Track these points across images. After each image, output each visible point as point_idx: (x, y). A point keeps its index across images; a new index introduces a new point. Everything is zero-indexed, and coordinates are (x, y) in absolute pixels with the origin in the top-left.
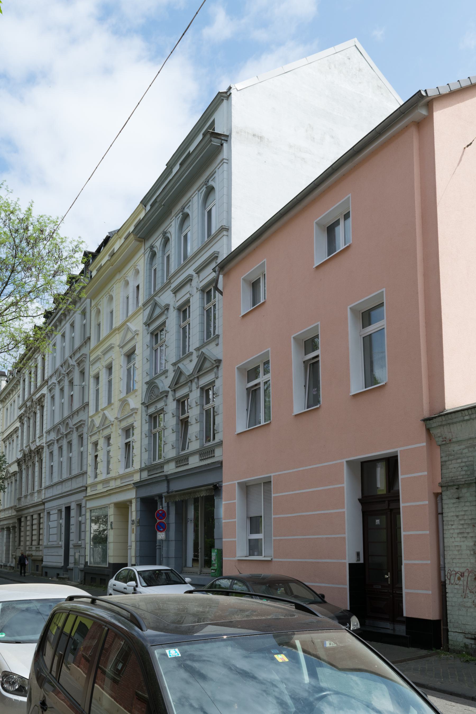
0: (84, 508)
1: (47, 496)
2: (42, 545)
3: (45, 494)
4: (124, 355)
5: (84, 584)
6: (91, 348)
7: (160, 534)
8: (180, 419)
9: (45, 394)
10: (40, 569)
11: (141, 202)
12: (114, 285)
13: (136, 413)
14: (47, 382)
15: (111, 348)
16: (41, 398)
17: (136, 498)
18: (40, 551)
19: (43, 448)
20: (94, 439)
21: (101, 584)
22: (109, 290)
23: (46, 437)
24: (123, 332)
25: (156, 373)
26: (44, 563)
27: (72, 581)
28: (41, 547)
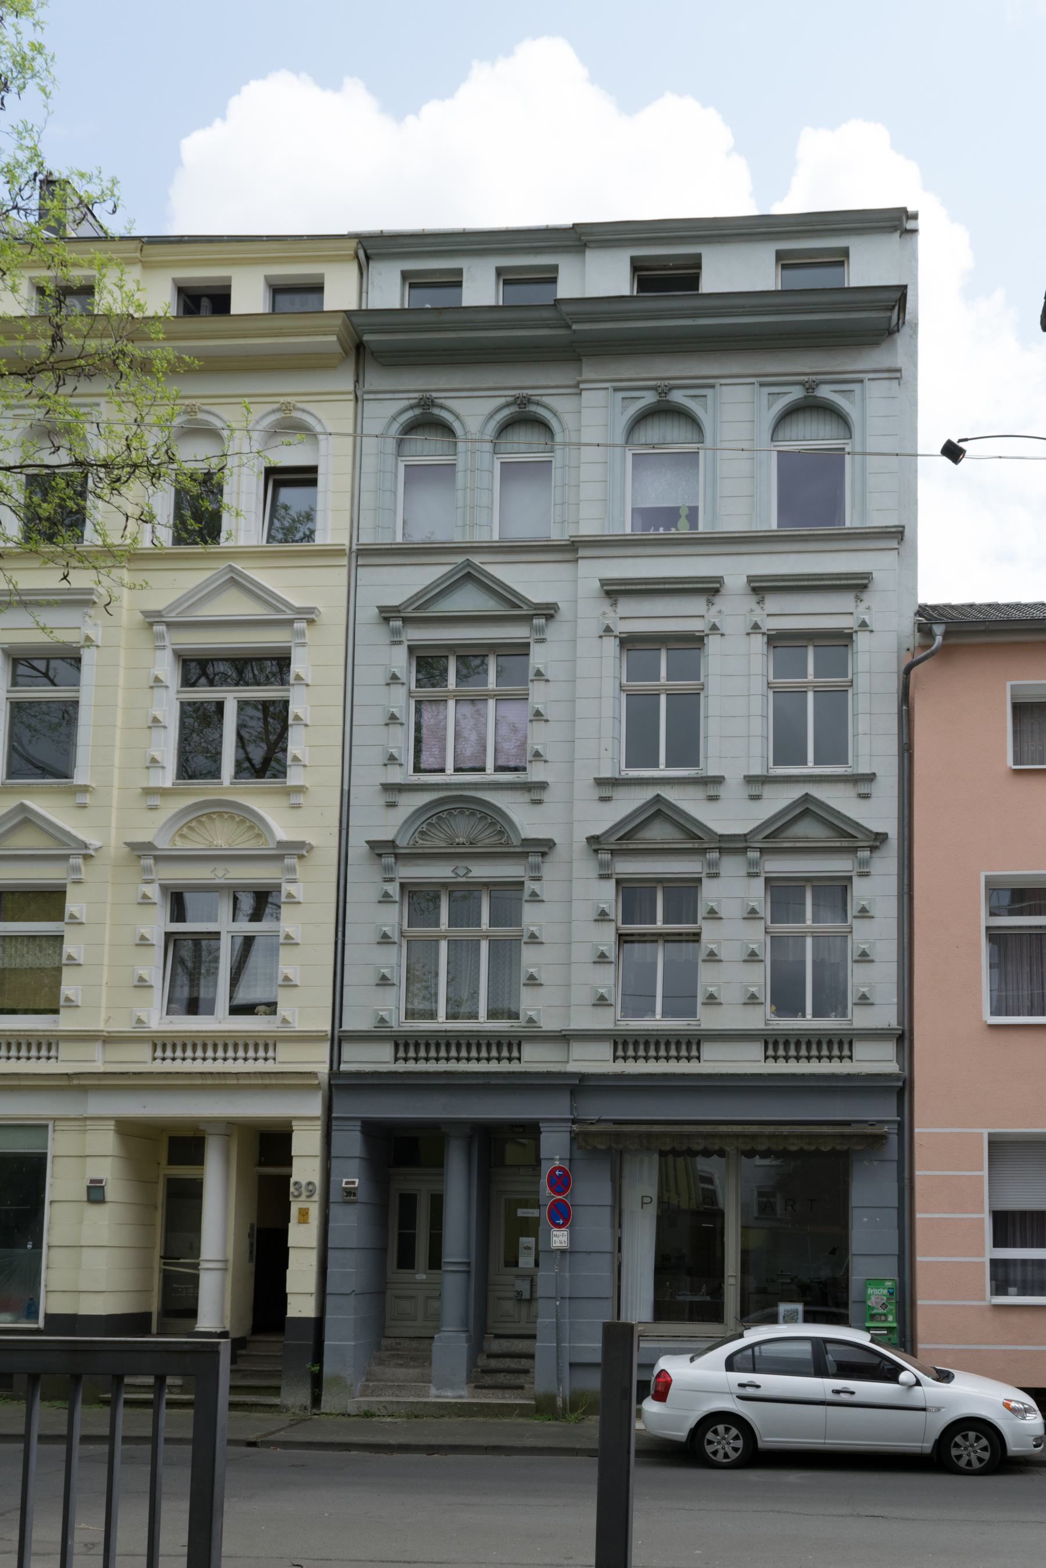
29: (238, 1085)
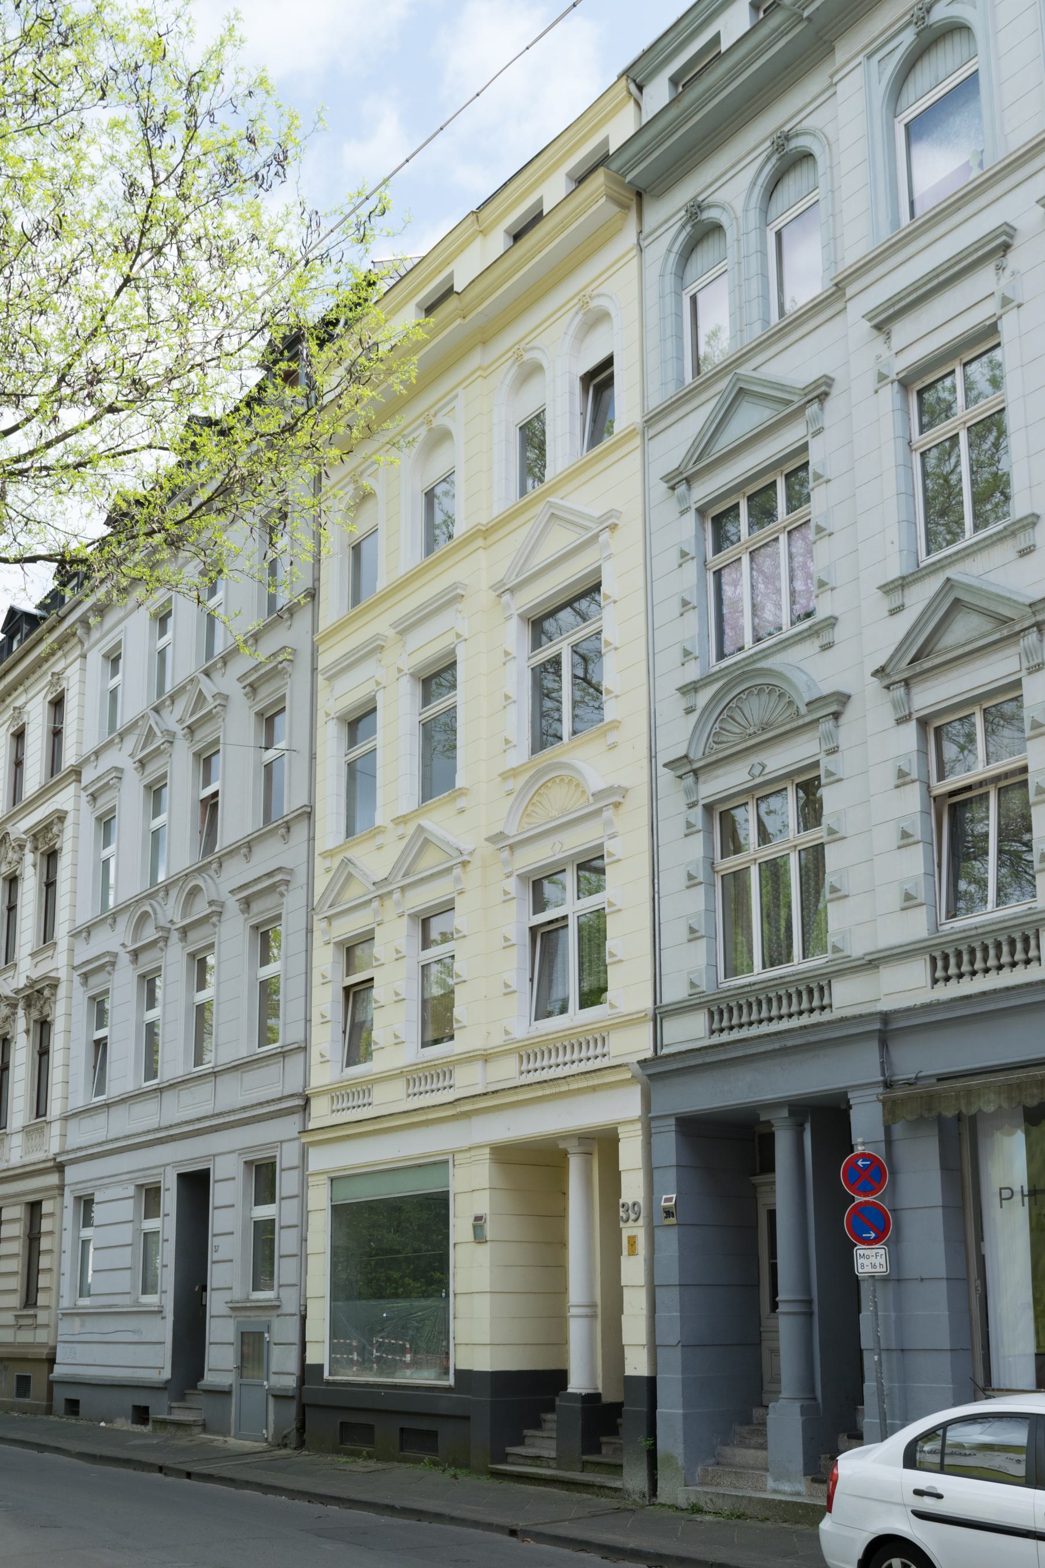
0: (295, 1174)
1: (73, 1142)
2: (48, 1307)
3: (64, 1135)
4: (520, 616)
5: (301, 1445)
6: (324, 625)
7: (867, 1252)
8: (935, 792)
9: (66, 812)
10: (38, 1388)
11: (626, 73)
12: (459, 390)
13: (617, 805)
14: (76, 772)
15: (452, 598)
16: (48, 828)
17: (649, 1122)
18: (37, 1327)
19: (54, 986)
20: (348, 927)
21: (402, 1450)
22: (432, 412)
23: (71, 950)
24: (524, 531)
25: (721, 655)
26: (58, 1371)
27: (225, 1433)
28: (43, 1317)
29: (569, 1091)
